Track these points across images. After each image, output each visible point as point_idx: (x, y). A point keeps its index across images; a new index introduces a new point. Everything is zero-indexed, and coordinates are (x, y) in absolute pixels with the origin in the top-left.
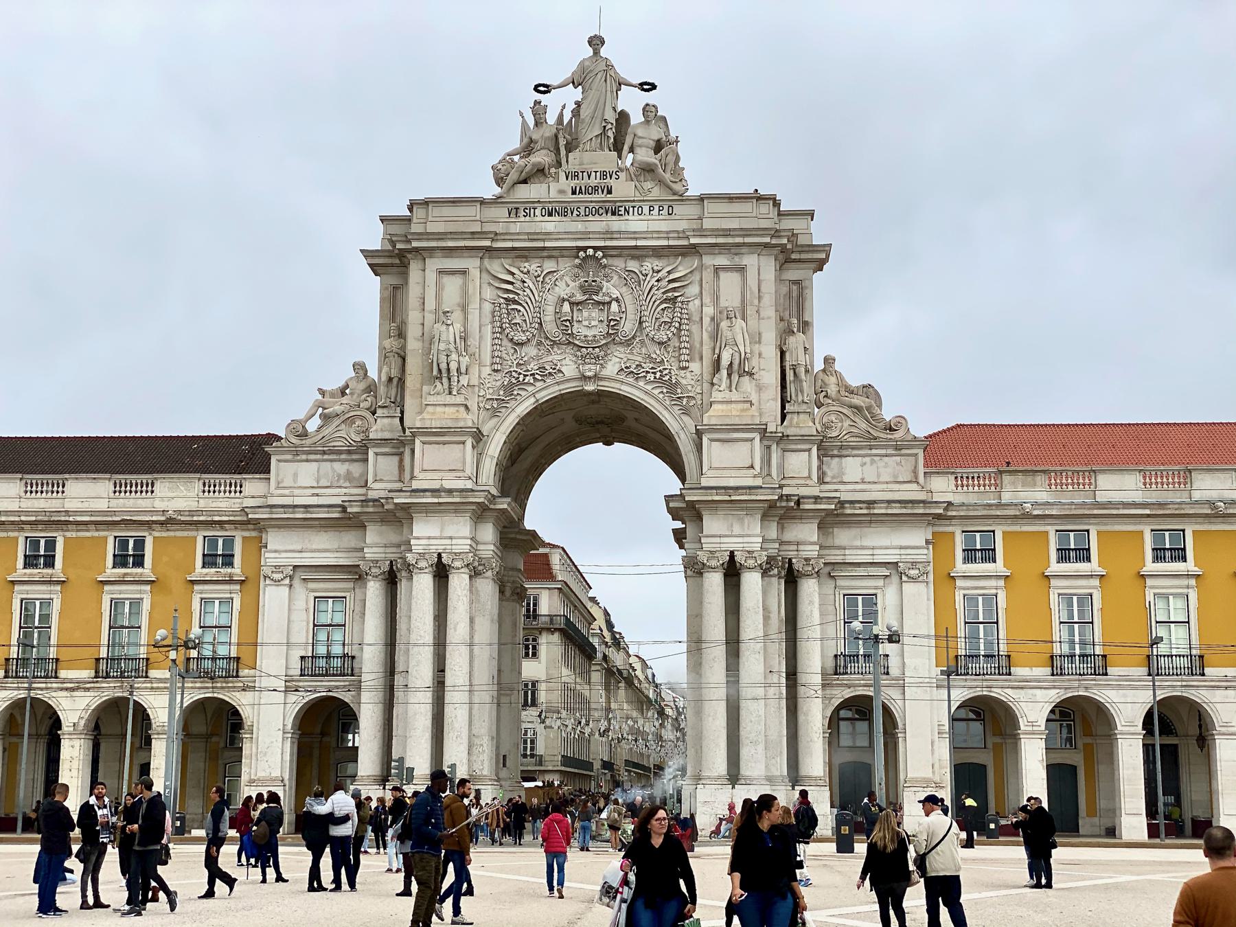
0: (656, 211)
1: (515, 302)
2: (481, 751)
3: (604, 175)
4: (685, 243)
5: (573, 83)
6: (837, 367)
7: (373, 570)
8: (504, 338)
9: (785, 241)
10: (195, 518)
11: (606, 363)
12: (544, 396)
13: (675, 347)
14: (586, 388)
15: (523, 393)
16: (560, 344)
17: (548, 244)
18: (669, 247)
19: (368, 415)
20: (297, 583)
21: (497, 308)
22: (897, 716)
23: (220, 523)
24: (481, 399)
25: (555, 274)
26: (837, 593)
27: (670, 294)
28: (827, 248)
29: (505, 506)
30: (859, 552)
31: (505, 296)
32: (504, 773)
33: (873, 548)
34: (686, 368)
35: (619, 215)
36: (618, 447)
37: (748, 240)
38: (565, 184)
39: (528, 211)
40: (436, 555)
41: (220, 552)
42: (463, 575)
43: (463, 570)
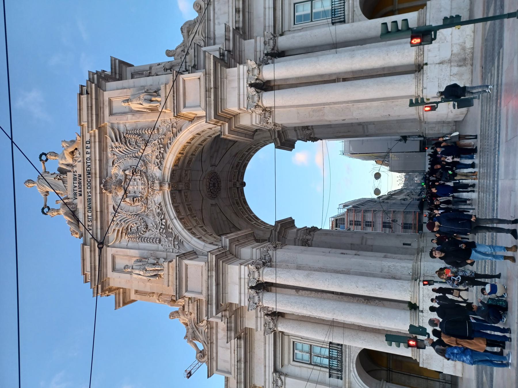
1: (127, 228)
2: (393, 268)
3: (75, 179)
5: (46, 195)
6: (173, 48)
7: (271, 326)
9: (95, 76)
11: (156, 177)
12: (172, 213)
15: (171, 226)
16: (147, 204)
17: (99, 210)
18: (100, 142)
20: (285, 370)
24: (174, 251)
26: (293, 29)
27: (123, 140)
28: (113, 59)
29: (228, 240)
30: (267, 17)
31: (124, 234)
32: (415, 245)
33: (265, 8)
34: (158, 129)
35: (90, 171)
36: (245, 180)
38: (79, 198)
39: (89, 220)
40: (250, 290)
42: (264, 272)
43: (261, 272)
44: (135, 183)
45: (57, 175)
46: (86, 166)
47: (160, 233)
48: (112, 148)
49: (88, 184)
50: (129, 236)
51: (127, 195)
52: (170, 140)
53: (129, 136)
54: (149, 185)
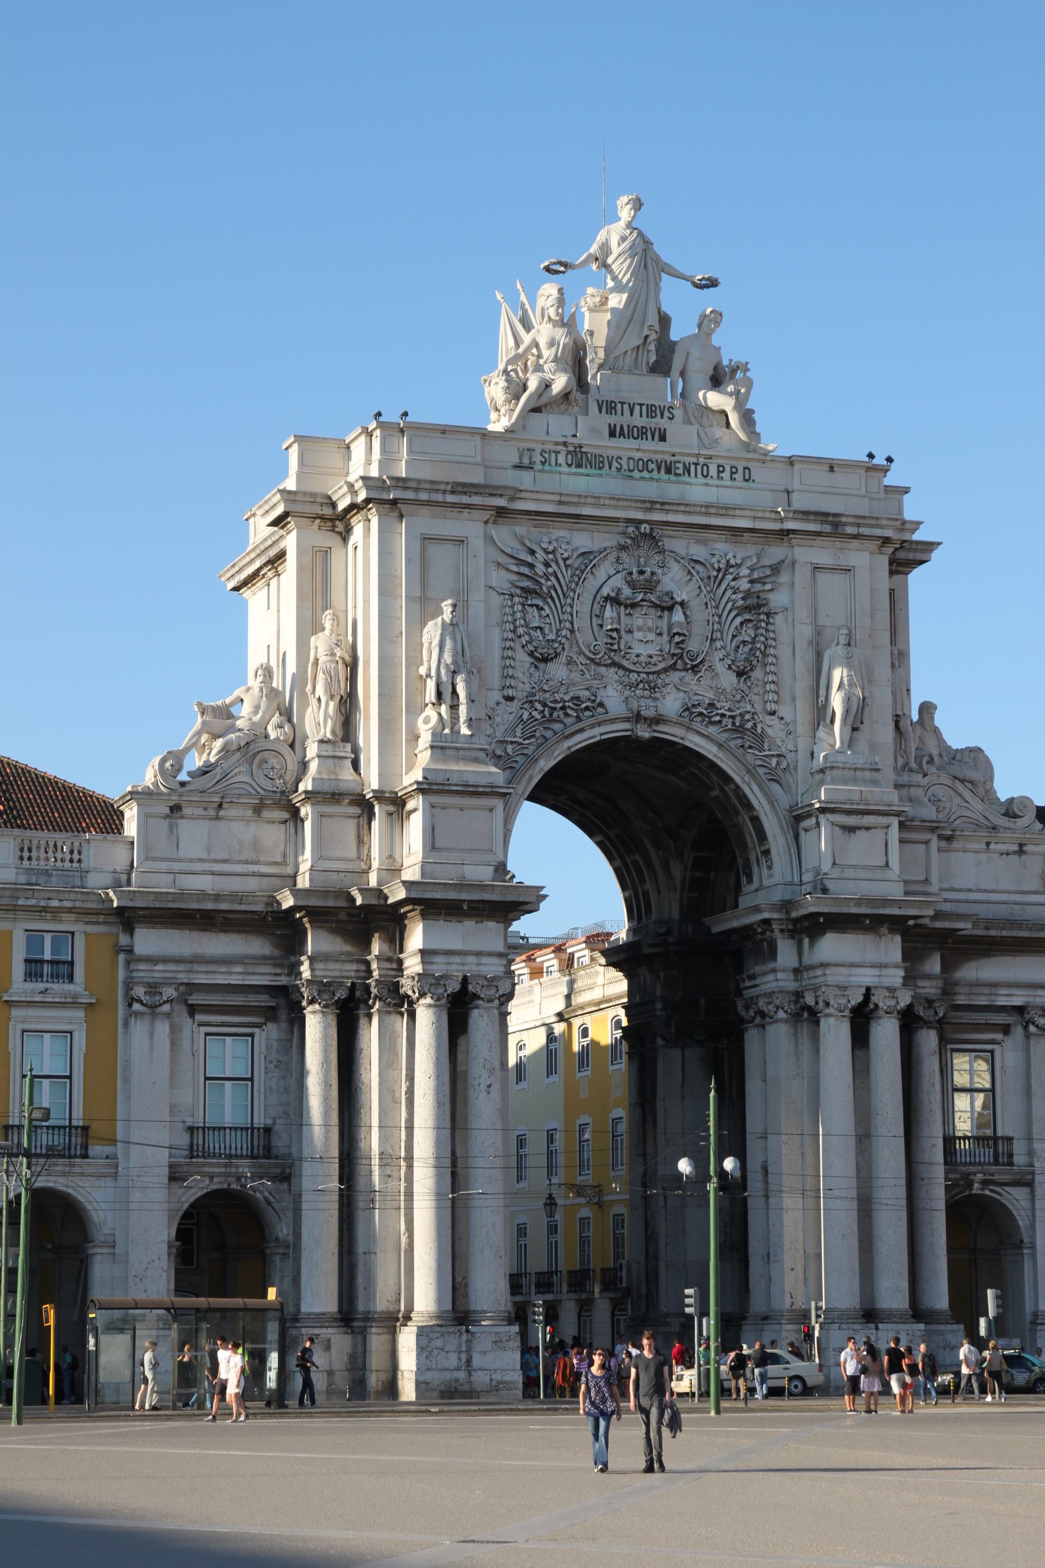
0: (726, 475)
3: (652, 411)
4: (777, 526)
8: (518, 647)
10: (21, 902)
13: (758, 680)
14: (640, 734)
16: (598, 664)
19: (286, 751)
21: (509, 603)
22: (1021, 1223)
23: (55, 912)
25: (592, 557)
28: (935, 546)
34: (773, 713)
35: (676, 475)
37: (866, 531)
41: (47, 956)
44: (651, 636)
45: (657, 332)
46: (688, 460)
47: (531, 702)
48: (738, 566)
49: (641, 462)
50: (517, 600)
51: (622, 608)
52: (750, 747)
53: (763, 624)
54: (643, 675)
